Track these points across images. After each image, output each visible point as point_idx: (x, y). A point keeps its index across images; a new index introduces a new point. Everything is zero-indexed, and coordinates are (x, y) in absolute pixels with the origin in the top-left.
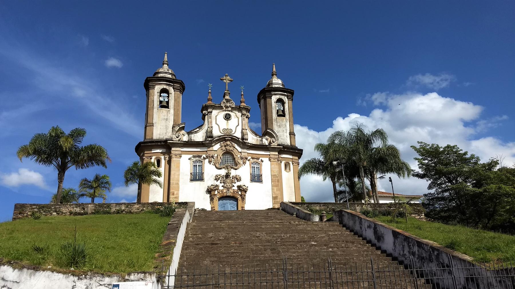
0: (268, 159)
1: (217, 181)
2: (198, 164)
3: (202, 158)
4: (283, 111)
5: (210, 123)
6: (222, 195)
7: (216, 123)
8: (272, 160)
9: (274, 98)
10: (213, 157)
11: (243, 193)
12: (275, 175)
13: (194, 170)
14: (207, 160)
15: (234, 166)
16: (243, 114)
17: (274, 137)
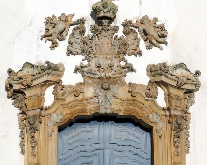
1: (54, 45)
6: (76, 111)
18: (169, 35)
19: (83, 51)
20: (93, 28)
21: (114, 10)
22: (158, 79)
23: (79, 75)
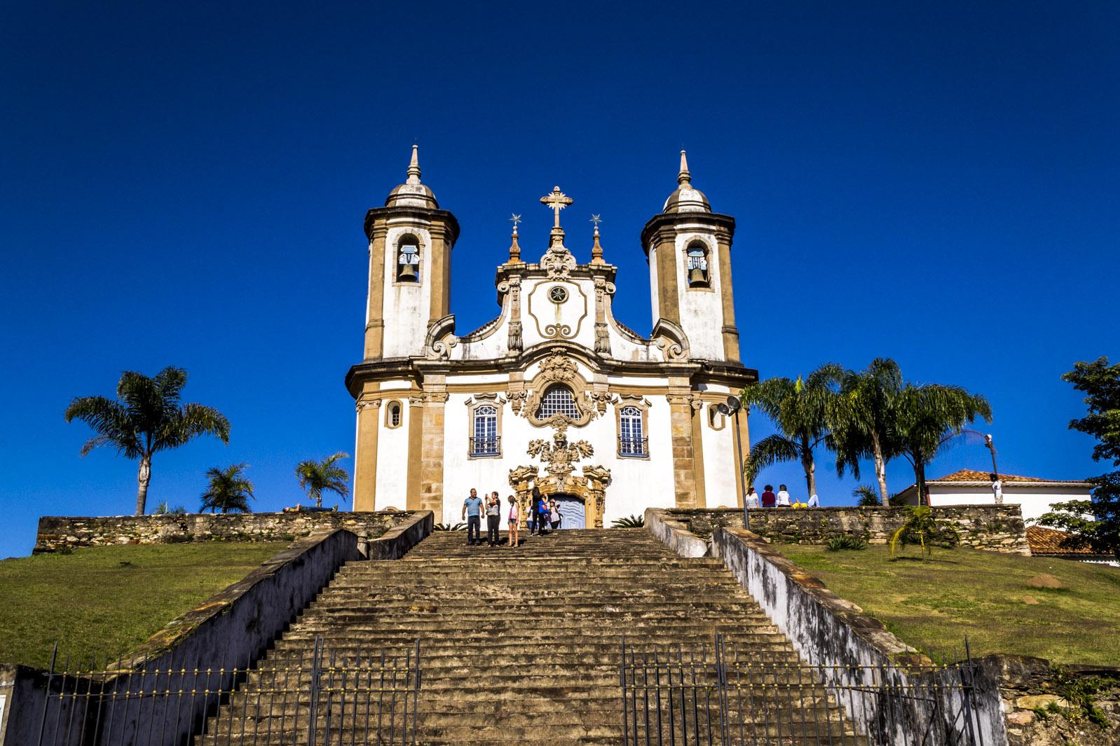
0: (664, 398)
2: (486, 416)
3: (497, 400)
4: (705, 273)
5: (516, 312)
7: (530, 313)
8: (674, 400)
9: (682, 241)
10: (523, 397)
11: (600, 486)
12: (682, 439)
13: (478, 430)
14: (509, 405)
15: (574, 420)
16: (596, 287)
17: (678, 342)
18: (594, 450)
19: (549, 459)
20: (554, 447)
21: (565, 438)
22: (588, 474)
23: (547, 472)
